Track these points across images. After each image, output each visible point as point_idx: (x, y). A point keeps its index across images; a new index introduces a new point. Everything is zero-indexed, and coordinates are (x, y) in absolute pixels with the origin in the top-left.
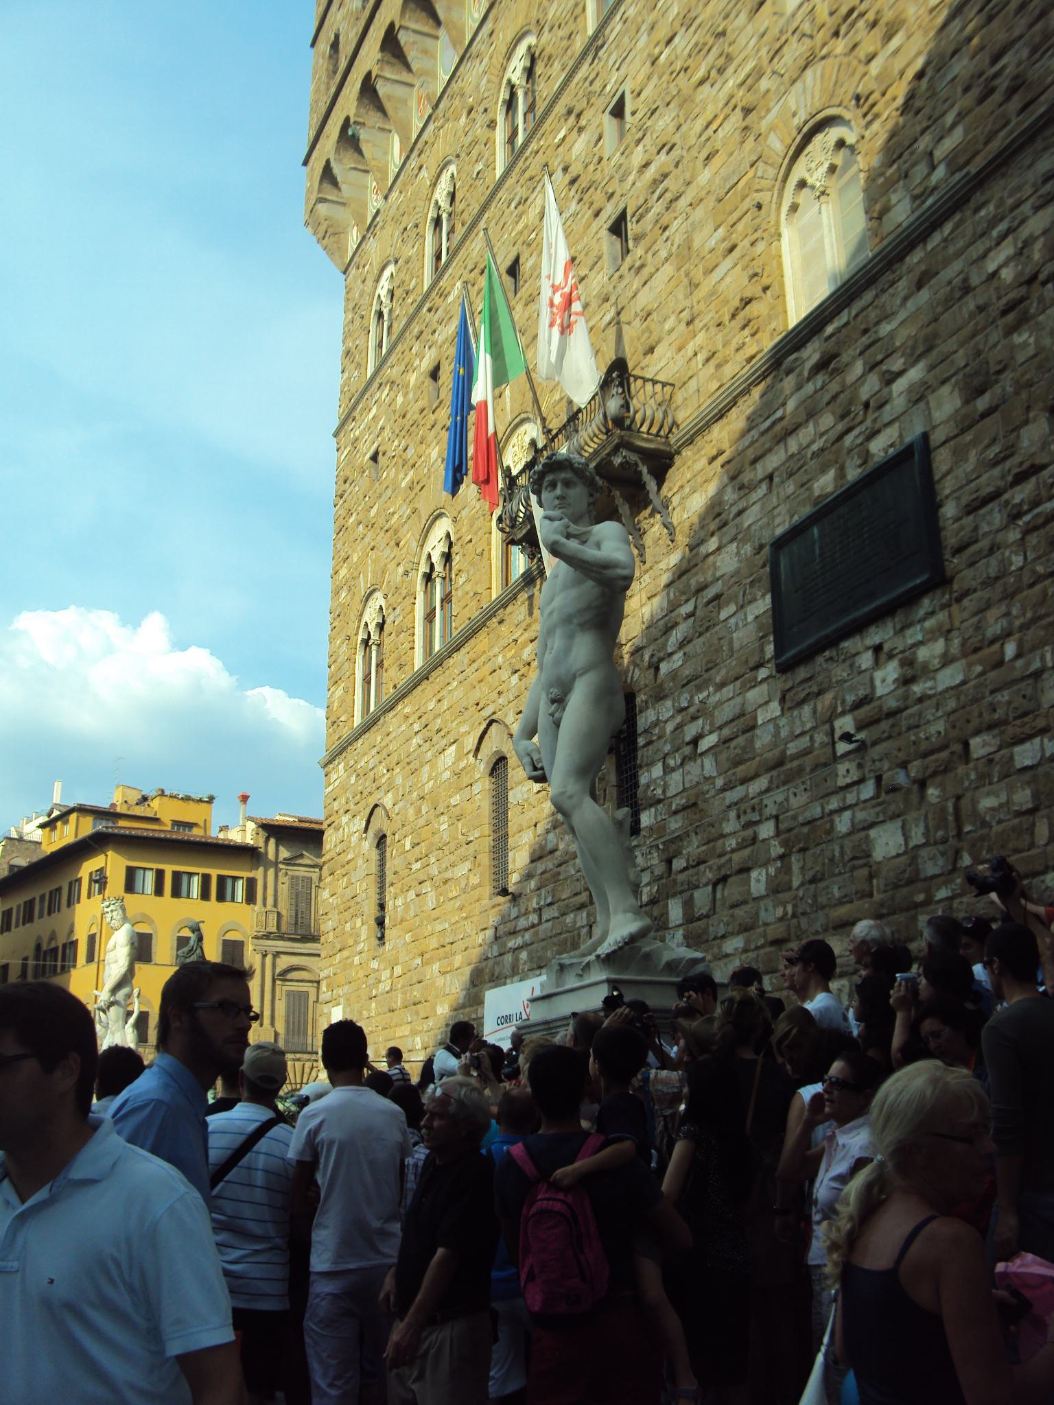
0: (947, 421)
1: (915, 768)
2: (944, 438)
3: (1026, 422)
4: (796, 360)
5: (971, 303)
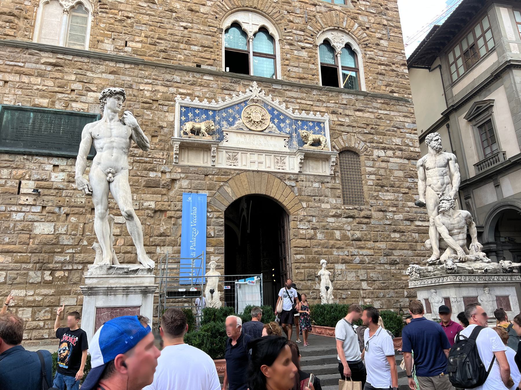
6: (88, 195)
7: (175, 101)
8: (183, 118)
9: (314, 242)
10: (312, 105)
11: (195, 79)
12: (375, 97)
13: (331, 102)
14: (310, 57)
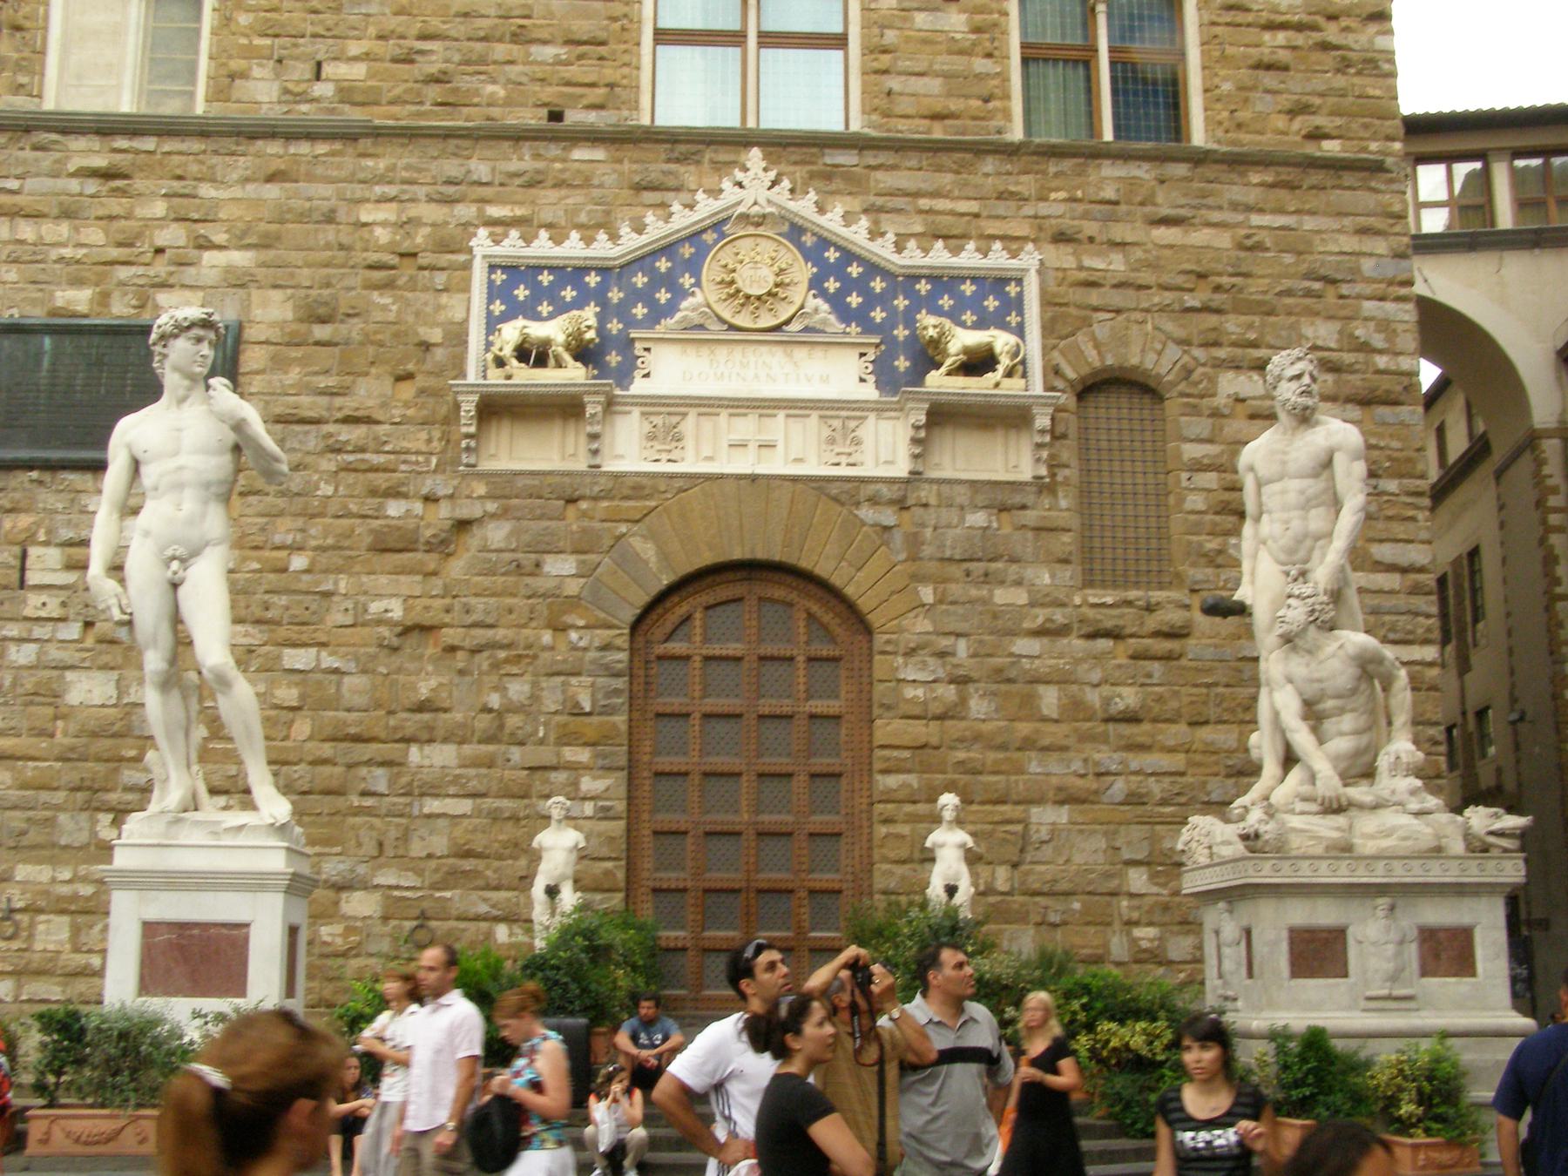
0: (272, 325)
2: (263, 338)
3: (367, 374)
4: (56, 142)
5: (329, 234)
6: (121, 623)
7: (470, 251)
8: (498, 308)
9: (954, 727)
10: (977, 216)
11: (540, 165)
12: (1238, 162)
13: (1053, 196)
14: (977, 30)
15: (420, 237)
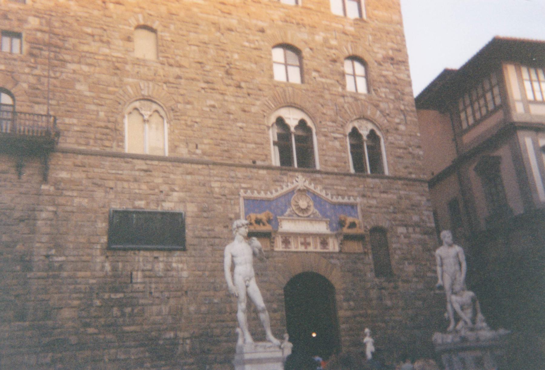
1: (166, 294)
5: (203, 189)
15: (226, 192)
